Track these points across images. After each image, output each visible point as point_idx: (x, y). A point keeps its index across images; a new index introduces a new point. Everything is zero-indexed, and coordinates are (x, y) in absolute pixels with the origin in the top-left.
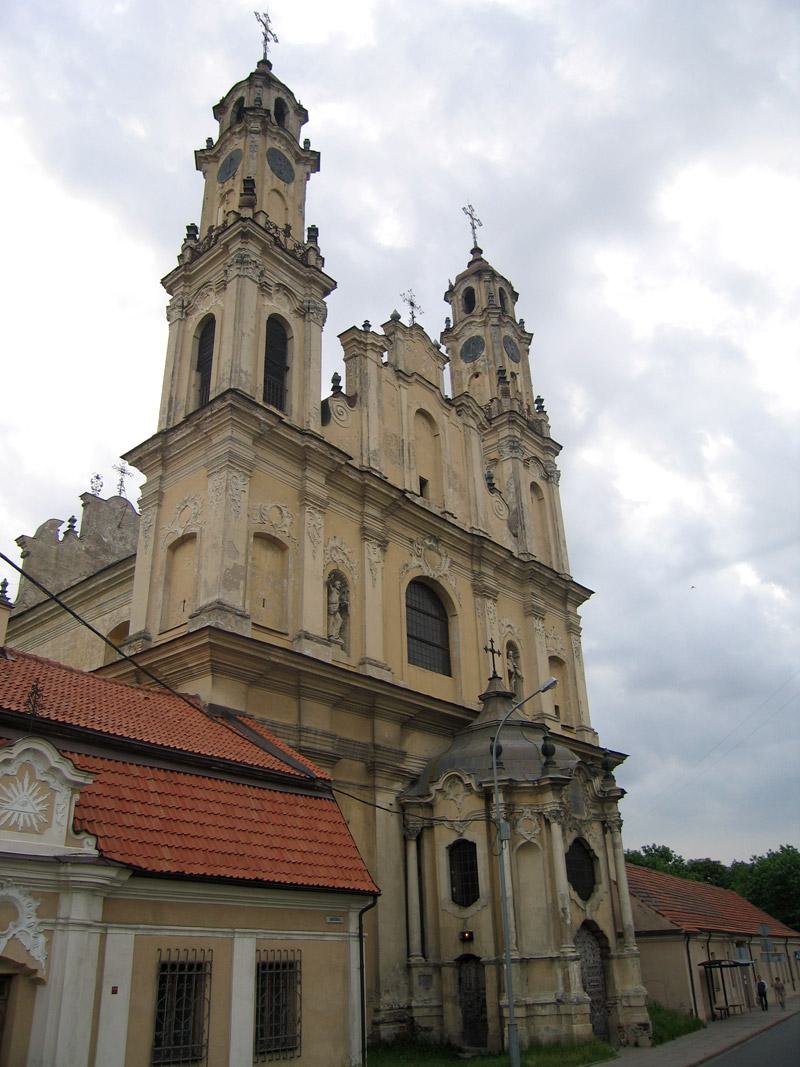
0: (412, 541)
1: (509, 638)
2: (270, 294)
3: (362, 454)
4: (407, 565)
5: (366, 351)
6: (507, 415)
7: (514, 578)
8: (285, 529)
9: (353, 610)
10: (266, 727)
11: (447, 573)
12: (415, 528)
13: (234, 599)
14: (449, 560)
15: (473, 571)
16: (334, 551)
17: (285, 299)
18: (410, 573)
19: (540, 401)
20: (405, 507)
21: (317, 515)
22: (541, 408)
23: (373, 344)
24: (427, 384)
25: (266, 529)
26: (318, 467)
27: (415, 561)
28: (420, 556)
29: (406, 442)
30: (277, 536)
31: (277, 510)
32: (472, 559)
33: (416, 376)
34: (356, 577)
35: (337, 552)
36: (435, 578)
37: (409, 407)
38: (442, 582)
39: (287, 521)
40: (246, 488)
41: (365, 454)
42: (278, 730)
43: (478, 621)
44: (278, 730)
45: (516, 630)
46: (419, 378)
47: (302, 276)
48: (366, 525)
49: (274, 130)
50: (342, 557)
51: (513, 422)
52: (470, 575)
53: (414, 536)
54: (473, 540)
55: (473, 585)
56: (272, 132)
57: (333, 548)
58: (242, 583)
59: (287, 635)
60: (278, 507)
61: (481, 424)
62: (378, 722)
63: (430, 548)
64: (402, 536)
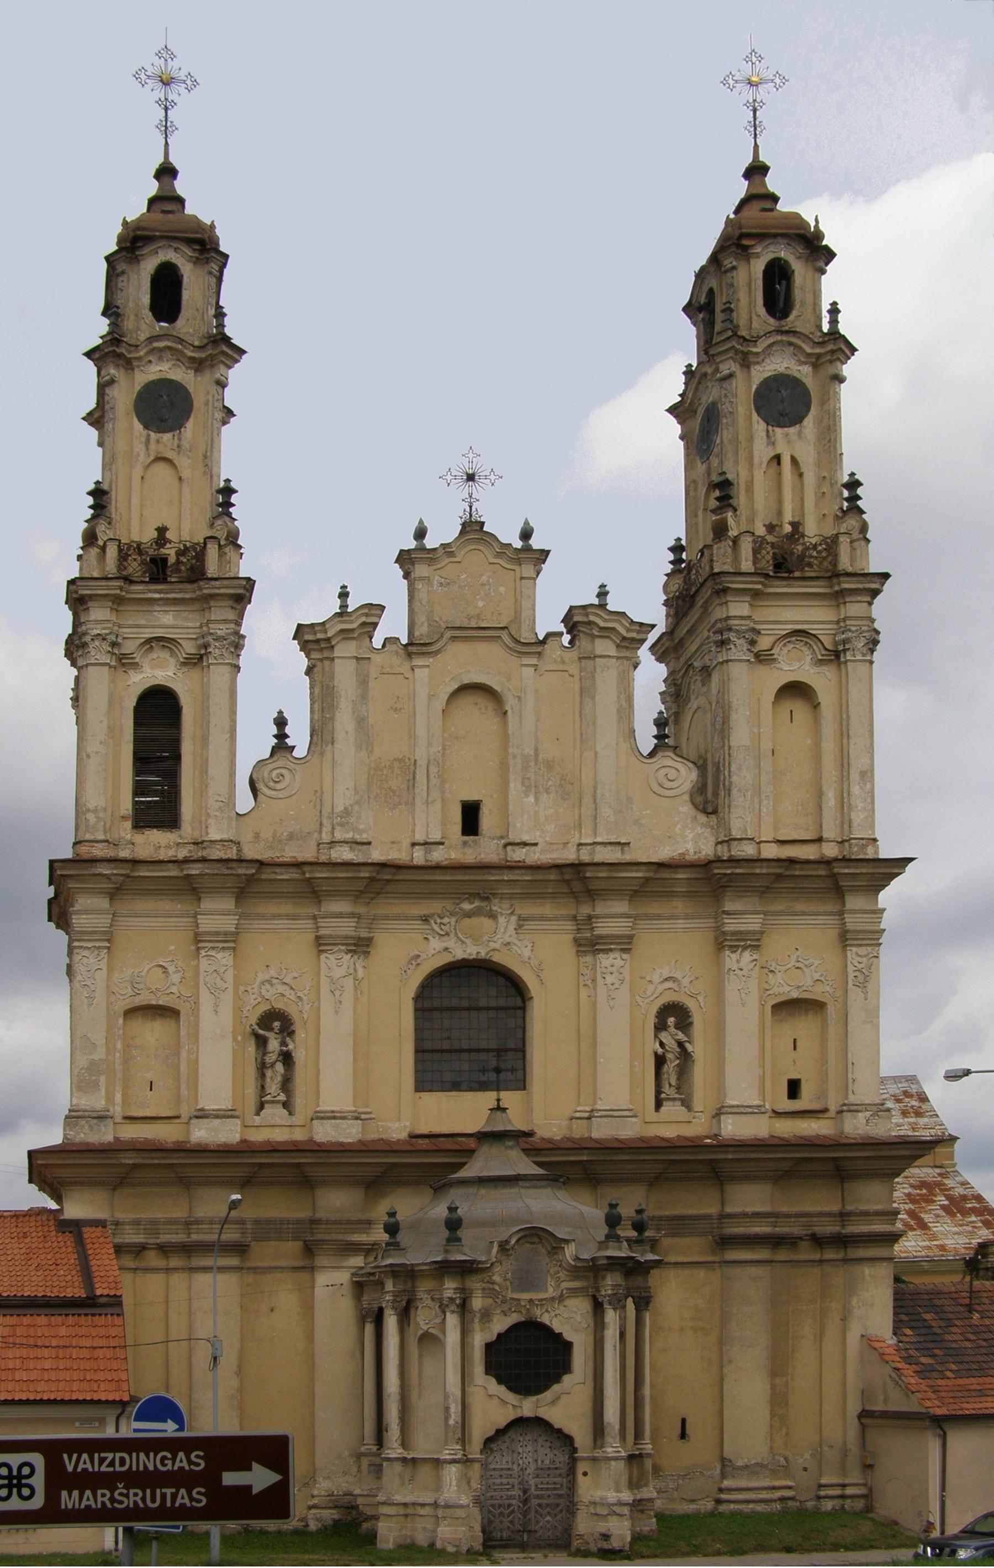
0: (425, 919)
1: (668, 998)
2: (136, 664)
3: (321, 824)
4: (418, 956)
5: (333, 647)
6: (709, 584)
7: (689, 895)
8: (174, 989)
9: (300, 1056)
10: (142, 1227)
11: (513, 939)
12: (433, 895)
13: (97, 1102)
14: (514, 918)
15: (574, 918)
16: (268, 986)
17: (164, 655)
18: (421, 967)
19: (853, 484)
20: (397, 878)
21: (219, 956)
22: (854, 498)
23: (342, 631)
24: (482, 633)
25: (145, 998)
26: (216, 891)
27: (436, 944)
28: (447, 934)
29: (422, 763)
30: (161, 1003)
31: (160, 970)
32: (576, 898)
33: (449, 634)
34: (307, 1007)
35: (272, 985)
36: (483, 955)
37: (431, 697)
38: (497, 958)
39: (176, 978)
40: (103, 965)
41: (325, 821)
42: (161, 1227)
43: (584, 993)
44: (161, 1227)
45: (686, 982)
46: (458, 633)
47: (192, 599)
48: (322, 932)
49: (142, 353)
50: (281, 989)
51: (725, 591)
52: (570, 926)
53: (434, 907)
54: (562, 874)
55: (576, 940)
56: (139, 359)
57: (263, 983)
58: (103, 1079)
59: (178, 1117)
60: (161, 966)
61: (624, 638)
62: (320, 1192)
63: (469, 915)
64: (406, 918)
